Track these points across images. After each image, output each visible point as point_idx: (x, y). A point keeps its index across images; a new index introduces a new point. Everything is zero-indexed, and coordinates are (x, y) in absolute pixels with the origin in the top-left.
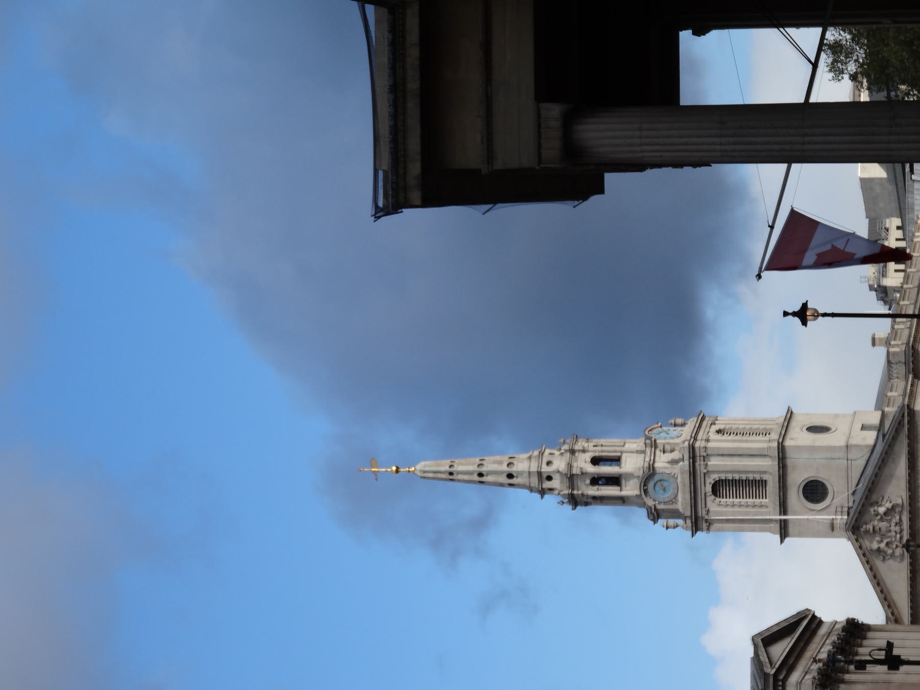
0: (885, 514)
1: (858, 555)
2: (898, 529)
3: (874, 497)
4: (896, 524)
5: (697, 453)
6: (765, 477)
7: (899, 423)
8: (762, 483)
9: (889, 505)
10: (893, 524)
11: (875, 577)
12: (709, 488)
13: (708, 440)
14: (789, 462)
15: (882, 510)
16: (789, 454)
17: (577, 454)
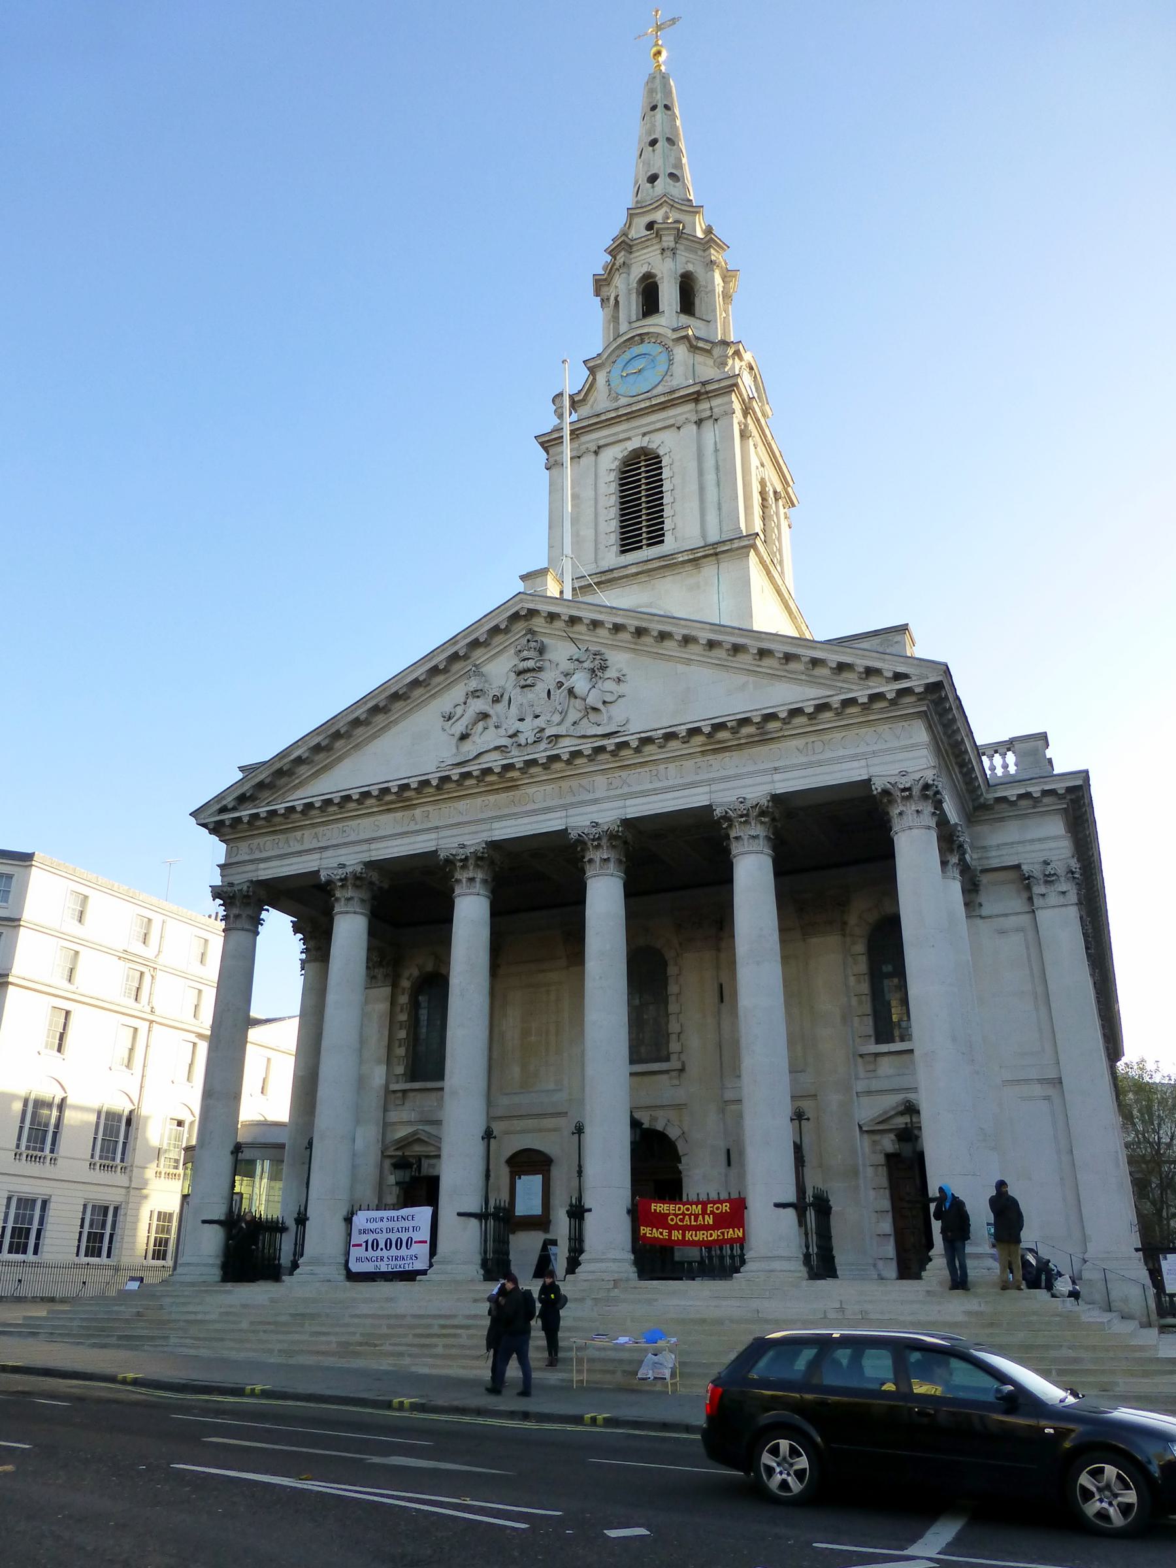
0: (571, 692)
1: (453, 640)
2: (527, 735)
3: (619, 660)
4: (542, 730)
5: (715, 402)
6: (668, 538)
7: (870, 672)
8: (657, 538)
9: (593, 699)
10: (540, 723)
11: (396, 697)
12: (635, 443)
13: (744, 435)
14: (709, 570)
15: (580, 682)
16: (728, 568)
17: (700, 253)
